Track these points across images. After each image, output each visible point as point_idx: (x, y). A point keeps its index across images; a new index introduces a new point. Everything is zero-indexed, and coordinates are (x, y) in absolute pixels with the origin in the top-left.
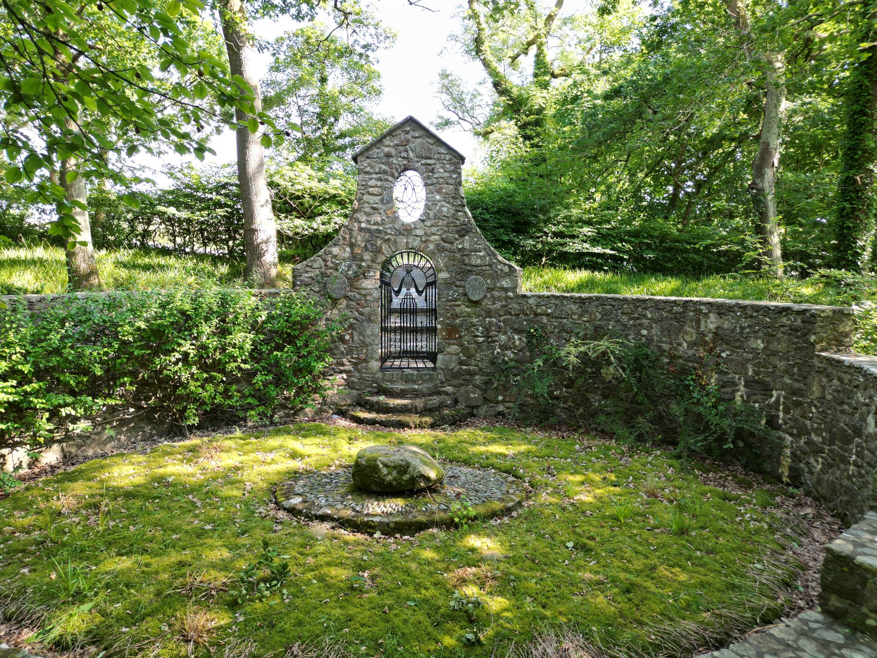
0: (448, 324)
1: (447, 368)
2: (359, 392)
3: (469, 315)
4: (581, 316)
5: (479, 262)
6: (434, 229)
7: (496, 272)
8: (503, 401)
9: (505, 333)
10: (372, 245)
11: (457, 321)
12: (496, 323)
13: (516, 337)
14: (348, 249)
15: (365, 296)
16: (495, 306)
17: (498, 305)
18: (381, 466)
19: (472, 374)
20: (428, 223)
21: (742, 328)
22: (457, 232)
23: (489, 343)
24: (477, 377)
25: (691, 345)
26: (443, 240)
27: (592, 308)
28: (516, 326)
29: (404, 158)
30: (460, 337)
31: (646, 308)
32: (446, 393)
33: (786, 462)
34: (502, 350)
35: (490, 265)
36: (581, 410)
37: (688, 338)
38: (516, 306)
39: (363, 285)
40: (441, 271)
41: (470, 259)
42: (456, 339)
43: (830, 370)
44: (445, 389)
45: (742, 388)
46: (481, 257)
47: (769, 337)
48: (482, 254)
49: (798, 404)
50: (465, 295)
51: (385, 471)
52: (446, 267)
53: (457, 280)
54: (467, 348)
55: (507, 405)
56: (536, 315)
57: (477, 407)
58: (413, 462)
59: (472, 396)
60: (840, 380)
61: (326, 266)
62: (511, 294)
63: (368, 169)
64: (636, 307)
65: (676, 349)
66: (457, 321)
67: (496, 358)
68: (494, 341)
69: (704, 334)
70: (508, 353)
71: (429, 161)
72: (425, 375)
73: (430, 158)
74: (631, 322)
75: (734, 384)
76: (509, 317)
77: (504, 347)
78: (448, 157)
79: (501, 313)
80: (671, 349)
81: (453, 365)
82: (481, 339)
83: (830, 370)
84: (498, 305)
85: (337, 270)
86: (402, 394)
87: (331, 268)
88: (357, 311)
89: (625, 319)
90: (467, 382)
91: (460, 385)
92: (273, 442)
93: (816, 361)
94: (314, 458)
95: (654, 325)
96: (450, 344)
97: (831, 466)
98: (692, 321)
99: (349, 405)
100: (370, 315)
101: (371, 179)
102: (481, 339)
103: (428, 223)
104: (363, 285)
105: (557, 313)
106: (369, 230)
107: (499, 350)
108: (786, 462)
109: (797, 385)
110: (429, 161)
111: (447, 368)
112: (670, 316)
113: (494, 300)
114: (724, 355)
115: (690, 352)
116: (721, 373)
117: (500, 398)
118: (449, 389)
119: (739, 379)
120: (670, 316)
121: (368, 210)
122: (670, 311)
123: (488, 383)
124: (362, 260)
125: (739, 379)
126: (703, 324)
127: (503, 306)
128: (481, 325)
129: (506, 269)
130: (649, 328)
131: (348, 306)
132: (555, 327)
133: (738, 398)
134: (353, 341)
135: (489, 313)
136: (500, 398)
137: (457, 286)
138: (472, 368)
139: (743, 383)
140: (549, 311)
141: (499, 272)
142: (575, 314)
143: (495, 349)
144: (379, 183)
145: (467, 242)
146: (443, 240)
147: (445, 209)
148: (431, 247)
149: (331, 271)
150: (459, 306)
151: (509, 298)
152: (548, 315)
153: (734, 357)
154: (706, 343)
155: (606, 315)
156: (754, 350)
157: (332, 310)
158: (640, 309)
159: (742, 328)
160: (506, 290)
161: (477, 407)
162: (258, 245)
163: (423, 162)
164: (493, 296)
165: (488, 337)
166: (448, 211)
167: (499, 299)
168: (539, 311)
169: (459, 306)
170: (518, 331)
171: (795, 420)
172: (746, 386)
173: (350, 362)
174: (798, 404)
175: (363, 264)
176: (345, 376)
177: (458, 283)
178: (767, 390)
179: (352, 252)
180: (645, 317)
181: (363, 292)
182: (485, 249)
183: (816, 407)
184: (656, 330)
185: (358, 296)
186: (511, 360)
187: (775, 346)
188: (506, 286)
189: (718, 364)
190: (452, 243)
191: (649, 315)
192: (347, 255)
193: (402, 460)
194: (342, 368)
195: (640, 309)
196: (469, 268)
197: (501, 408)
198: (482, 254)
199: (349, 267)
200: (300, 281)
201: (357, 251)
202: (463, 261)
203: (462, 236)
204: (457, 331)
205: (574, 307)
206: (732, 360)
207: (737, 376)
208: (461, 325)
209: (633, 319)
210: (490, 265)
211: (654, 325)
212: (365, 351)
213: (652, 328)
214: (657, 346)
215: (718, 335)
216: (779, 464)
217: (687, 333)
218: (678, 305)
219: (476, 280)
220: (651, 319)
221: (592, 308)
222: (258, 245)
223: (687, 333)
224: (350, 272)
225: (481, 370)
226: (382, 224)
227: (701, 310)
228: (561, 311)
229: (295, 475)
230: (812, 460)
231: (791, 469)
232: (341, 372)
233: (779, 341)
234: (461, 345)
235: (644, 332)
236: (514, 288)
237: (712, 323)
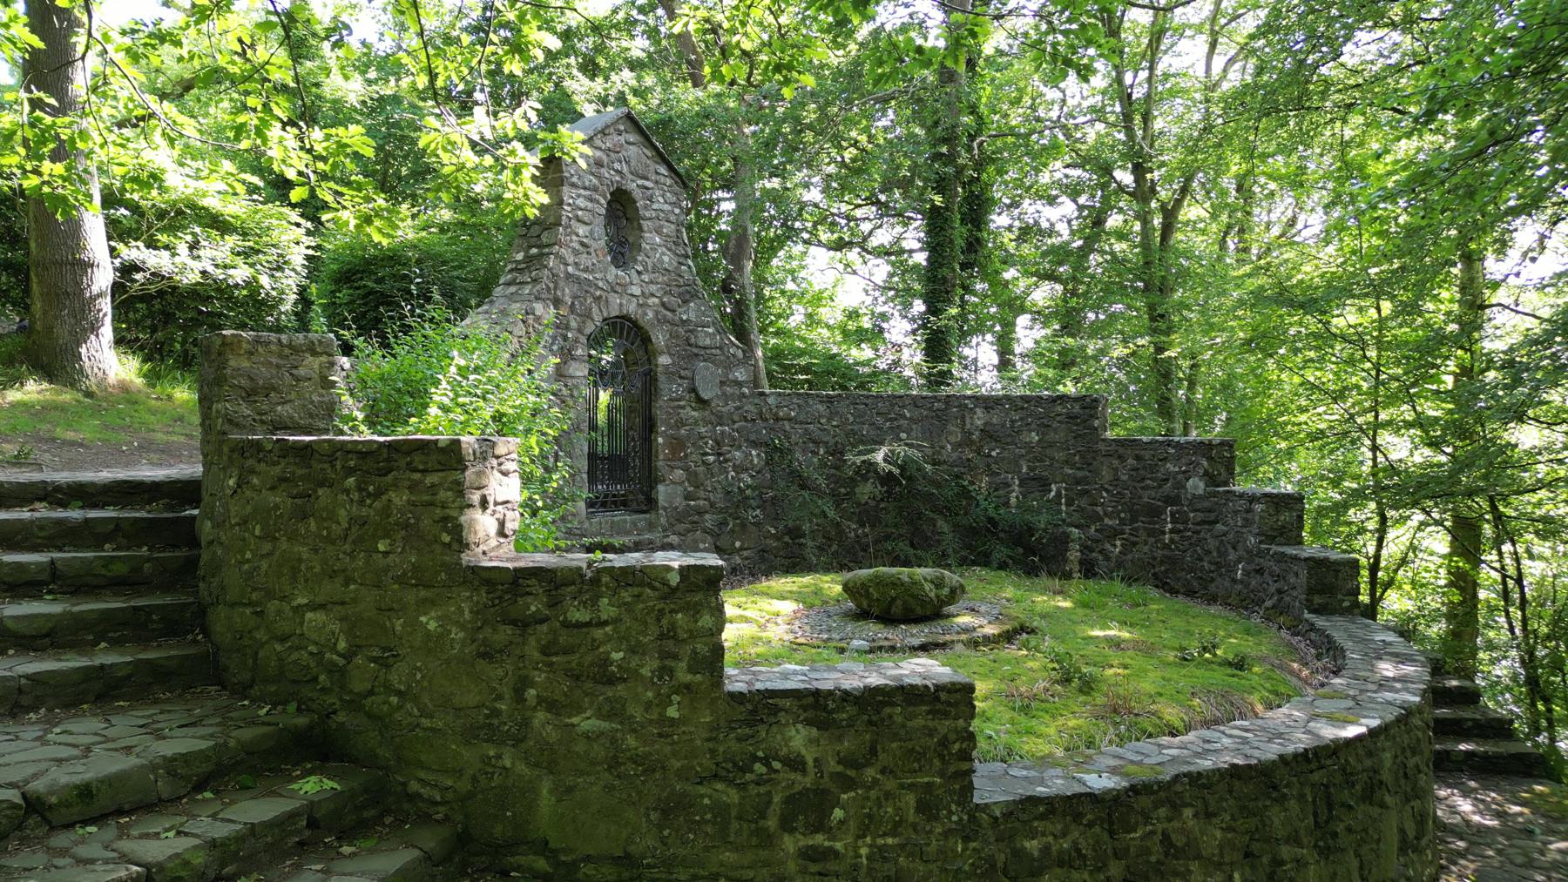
0: (672, 436)
3: (696, 423)
4: (830, 419)
5: (708, 342)
6: (653, 288)
8: (741, 549)
10: (581, 304)
19: (700, 512)
20: (646, 278)
21: (1013, 421)
22: (680, 295)
24: (707, 516)
25: (956, 446)
26: (663, 304)
27: (842, 407)
28: (753, 437)
29: (617, 171)
31: (903, 407)
33: (1074, 555)
35: (720, 348)
36: (834, 547)
37: (952, 439)
38: (752, 408)
42: (680, 459)
43: (1121, 450)
47: (1044, 428)
49: (1085, 492)
50: (693, 390)
51: (927, 586)
54: (696, 473)
55: (745, 553)
56: (777, 419)
60: (1138, 458)
63: (574, 179)
64: (892, 405)
68: (726, 461)
70: (744, 476)
71: (647, 184)
73: (647, 179)
77: (739, 469)
78: (669, 181)
79: (736, 418)
81: (679, 502)
83: (1121, 450)
89: (880, 420)
93: (1101, 446)
97: (1134, 544)
101: (579, 196)
102: (711, 458)
103: (646, 278)
105: (801, 418)
106: (578, 278)
108: (1074, 555)
109: (1080, 474)
110: (647, 184)
113: (726, 397)
116: (993, 474)
117: (738, 544)
121: (577, 246)
122: (930, 409)
123: (724, 523)
124: (568, 328)
126: (968, 421)
127: (738, 408)
129: (740, 354)
133: (1013, 501)
136: (738, 544)
138: (702, 502)
144: (590, 205)
145: (690, 313)
146: (663, 304)
147: (666, 259)
148: (651, 315)
150: (683, 407)
151: (743, 395)
152: (790, 420)
153: (1006, 454)
154: (972, 442)
156: (1028, 446)
159: (1013, 421)
162: (94, 298)
163: (640, 182)
164: (724, 394)
165: (720, 454)
166: (670, 263)
167: (732, 397)
169: (683, 407)
170: (754, 444)
171: (1081, 510)
172: (1020, 486)
174: (1085, 492)
178: (1045, 485)
183: (1107, 491)
186: (748, 487)
187: (1052, 436)
190: (673, 311)
196: (695, 350)
197: (738, 560)
202: (688, 339)
203: (685, 302)
204: (683, 447)
205: (821, 408)
206: (1003, 459)
208: (688, 437)
209: (891, 420)
210: (720, 348)
215: (988, 434)
216: (1066, 560)
217: (950, 433)
221: (842, 407)
222: (94, 298)
223: (950, 433)
225: (712, 505)
226: (592, 272)
230: (1108, 546)
231: (1081, 563)
233: (1055, 430)
234: (687, 469)
237: (979, 418)
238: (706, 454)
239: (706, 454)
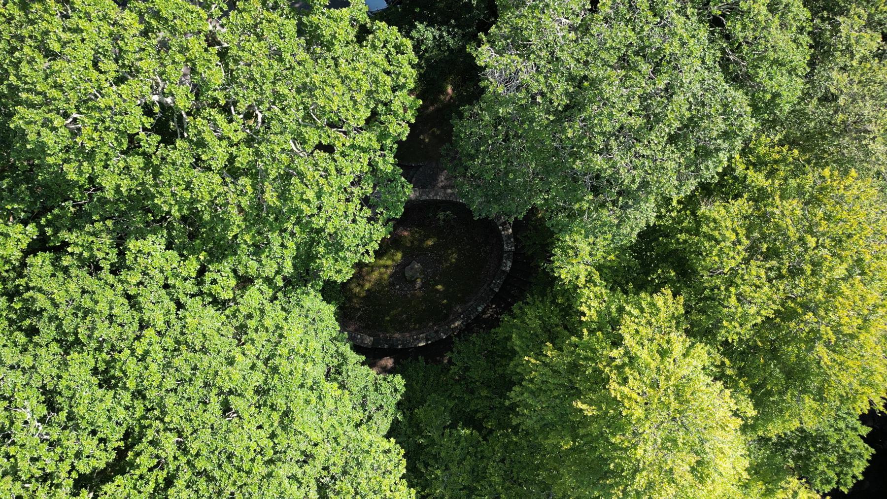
229: (391, 276)
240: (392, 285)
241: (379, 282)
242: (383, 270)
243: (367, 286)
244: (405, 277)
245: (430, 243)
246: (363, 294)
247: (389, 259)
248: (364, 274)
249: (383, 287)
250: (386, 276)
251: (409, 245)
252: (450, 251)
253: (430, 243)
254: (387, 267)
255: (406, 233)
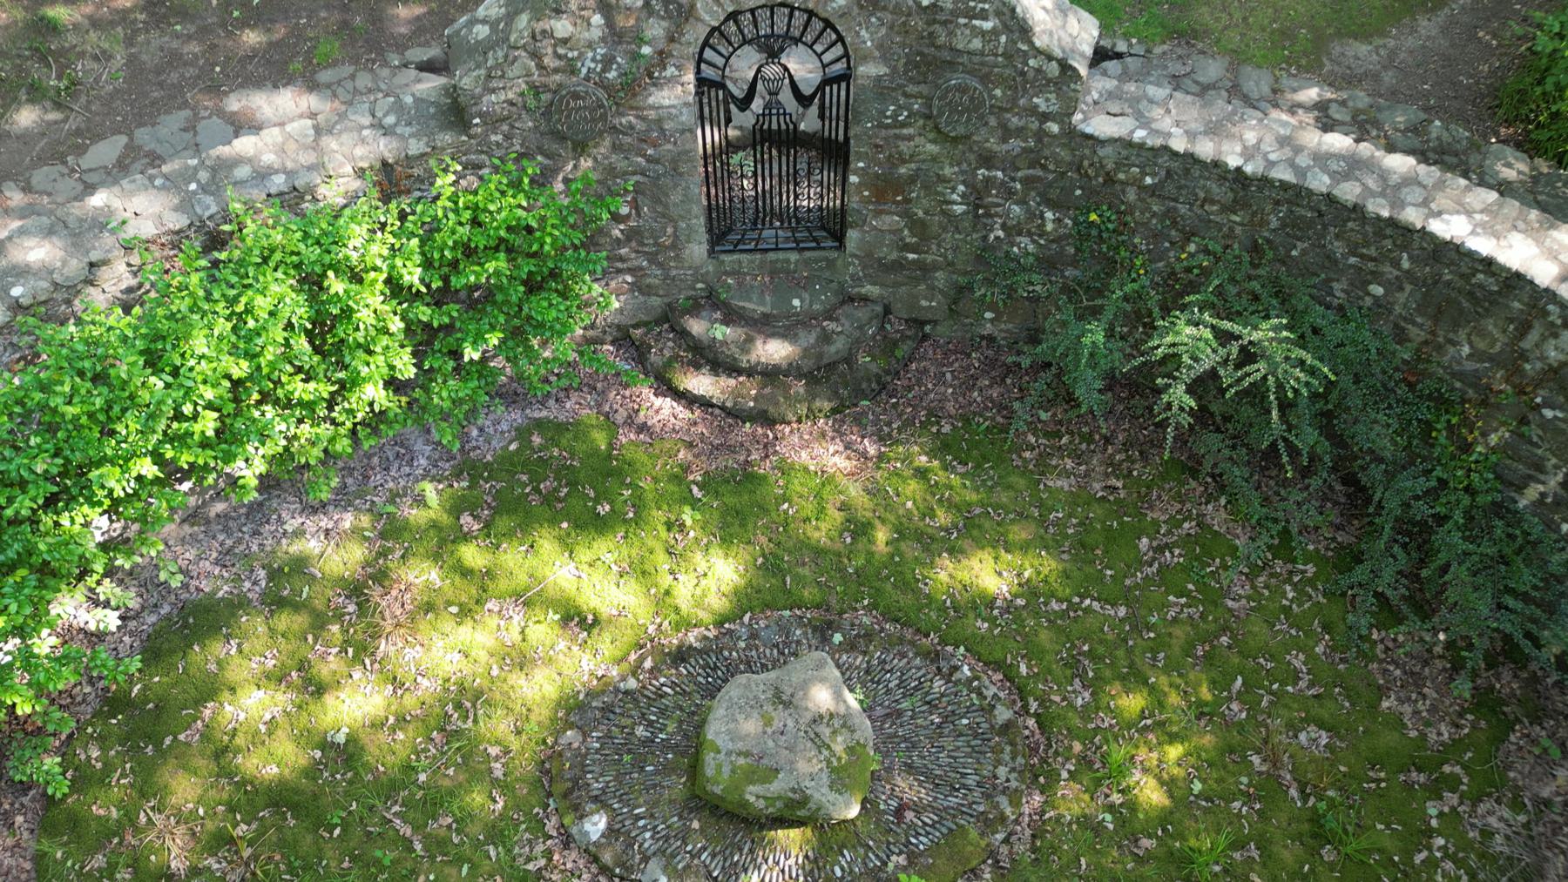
0: (877, 176)
1: (869, 255)
2: (666, 300)
3: (934, 159)
5: (977, 44)
7: (1023, 74)
9: (1022, 202)
11: (903, 170)
12: (1003, 183)
13: (1049, 215)
14: (597, 19)
15: (659, 121)
16: (1005, 147)
17: (1015, 144)
18: (752, 799)
19: (925, 269)
23: (977, 216)
28: (1054, 194)
30: (907, 201)
31: (1404, 248)
32: (865, 299)
34: (1008, 235)
39: (651, 100)
40: (865, 59)
41: (951, 34)
44: (863, 291)
45: (1552, 483)
46: (983, 33)
48: (987, 25)
52: (880, 47)
53: (911, 80)
57: (935, 323)
58: (817, 796)
59: (924, 303)
61: (540, 67)
62: (1054, 128)
65: (1439, 348)
66: (903, 170)
67: (993, 248)
69: (1524, 356)
72: (816, 261)
74: (1352, 260)
75: (1540, 468)
76: (1040, 173)
77: (1012, 231)
80: (1426, 343)
82: (959, 209)
84: (1015, 144)
85: (573, 71)
86: (766, 326)
87: (556, 71)
88: (643, 156)
90: (916, 281)
91: (897, 285)
92: (512, 558)
94: (607, 637)
95: (1408, 288)
96: (881, 212)
98: (1511, 320)
99: (645, 324)
100: (675, 161)
104: (651, 100)
105: (1170, 188)
107: (1001, 234)
111: (869, 255)
112: (1460, 283)
114: (1548, 413)
115: (1469, 366)
118: (871, 290)
119: (1556, 467)
120: (1460, 283)
123: (962, 291)
125: (1556, 467)
126: (1533, 336)
128: (964, 183)
130: (1394, 286)
131: (616, 148)
132: (1154, 215)
134: (638, 215)
135: (987, 160)
137: (906, 95)
139: (1560, 477)
140: (1148, 180)
141: (1031, 74)
142: (1213, 202)
143: (992, 230)
149: (557, 77)
150: (910, 138)
152: (1142, 188)
154: (1518, 370)
155: (1294, 227)
157: (577, 159)
158: (1388, 244)
160: (1045, 117)
161: (935, 323)
167: (1020, 132)
168: (1121, 176)
169: (910, 138)
173: (637, 252)
175: (646, 50)
176: (629, 279)
177: (911, 89)
179: (610, 23)
180: (1396, 264)
181: (652, 114)
182: (998, 14)
184: (1404, 300)
185: (640, 126)
188: (1043, 108)
189: (1524, 421)
191: (1406, 265)
192: (596, 33)
193: (793, 790)
194: (619, 265)
195: (1388, 244)
198: (987, 25)
199: (608, 62)
200: (480, 115)
201: (625, 22)
207: (1554, 461)
208: (912, 180)
209: (1362, 256)
211: (1408, 288)
212: (670, 230)
213: (1401, 289)
214: (1396, 326)
217: (1483, 334)
218: (1494, 274)
219: (963, 89)
220: (1408, 272)
223: (1483, 334)
224: (612, 75)
227: (1546, 313)
228: (1180, 188)
229: (578, 709)
232: (619, 271)
234: (907, 215)
235: (1378, 290)
236: (1064, 116)
238: (955, 203)
239: (955, 203)
240: (557, 783)
241: (455, 713)
242: (543, 631)
243: (354, 705)
244: (692, 747)
245: (988, 574)
246: (273, 762)
247: (641, 571)
248: (389, 605)
249: (471, 761)
250: (539, 689)
251: (822, 532)
252: (1133, 703)
253: (988, 574)
254: (577, 620)
255: (833, 458)
